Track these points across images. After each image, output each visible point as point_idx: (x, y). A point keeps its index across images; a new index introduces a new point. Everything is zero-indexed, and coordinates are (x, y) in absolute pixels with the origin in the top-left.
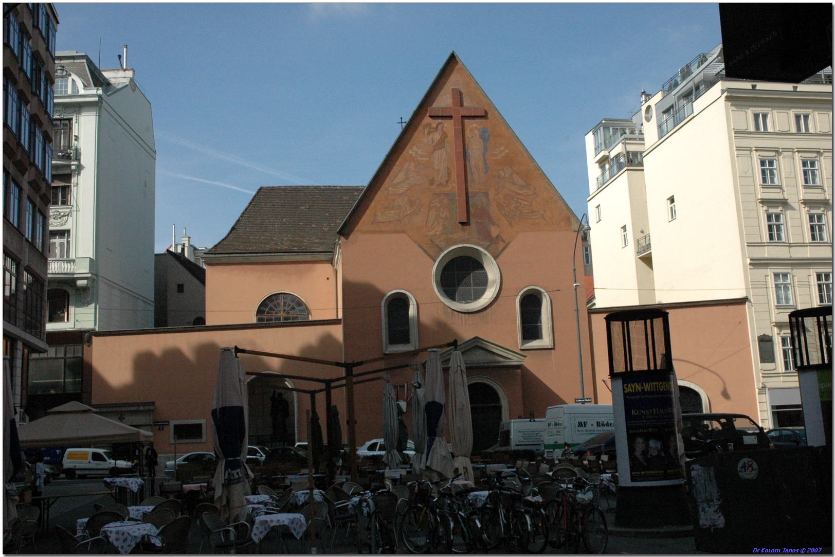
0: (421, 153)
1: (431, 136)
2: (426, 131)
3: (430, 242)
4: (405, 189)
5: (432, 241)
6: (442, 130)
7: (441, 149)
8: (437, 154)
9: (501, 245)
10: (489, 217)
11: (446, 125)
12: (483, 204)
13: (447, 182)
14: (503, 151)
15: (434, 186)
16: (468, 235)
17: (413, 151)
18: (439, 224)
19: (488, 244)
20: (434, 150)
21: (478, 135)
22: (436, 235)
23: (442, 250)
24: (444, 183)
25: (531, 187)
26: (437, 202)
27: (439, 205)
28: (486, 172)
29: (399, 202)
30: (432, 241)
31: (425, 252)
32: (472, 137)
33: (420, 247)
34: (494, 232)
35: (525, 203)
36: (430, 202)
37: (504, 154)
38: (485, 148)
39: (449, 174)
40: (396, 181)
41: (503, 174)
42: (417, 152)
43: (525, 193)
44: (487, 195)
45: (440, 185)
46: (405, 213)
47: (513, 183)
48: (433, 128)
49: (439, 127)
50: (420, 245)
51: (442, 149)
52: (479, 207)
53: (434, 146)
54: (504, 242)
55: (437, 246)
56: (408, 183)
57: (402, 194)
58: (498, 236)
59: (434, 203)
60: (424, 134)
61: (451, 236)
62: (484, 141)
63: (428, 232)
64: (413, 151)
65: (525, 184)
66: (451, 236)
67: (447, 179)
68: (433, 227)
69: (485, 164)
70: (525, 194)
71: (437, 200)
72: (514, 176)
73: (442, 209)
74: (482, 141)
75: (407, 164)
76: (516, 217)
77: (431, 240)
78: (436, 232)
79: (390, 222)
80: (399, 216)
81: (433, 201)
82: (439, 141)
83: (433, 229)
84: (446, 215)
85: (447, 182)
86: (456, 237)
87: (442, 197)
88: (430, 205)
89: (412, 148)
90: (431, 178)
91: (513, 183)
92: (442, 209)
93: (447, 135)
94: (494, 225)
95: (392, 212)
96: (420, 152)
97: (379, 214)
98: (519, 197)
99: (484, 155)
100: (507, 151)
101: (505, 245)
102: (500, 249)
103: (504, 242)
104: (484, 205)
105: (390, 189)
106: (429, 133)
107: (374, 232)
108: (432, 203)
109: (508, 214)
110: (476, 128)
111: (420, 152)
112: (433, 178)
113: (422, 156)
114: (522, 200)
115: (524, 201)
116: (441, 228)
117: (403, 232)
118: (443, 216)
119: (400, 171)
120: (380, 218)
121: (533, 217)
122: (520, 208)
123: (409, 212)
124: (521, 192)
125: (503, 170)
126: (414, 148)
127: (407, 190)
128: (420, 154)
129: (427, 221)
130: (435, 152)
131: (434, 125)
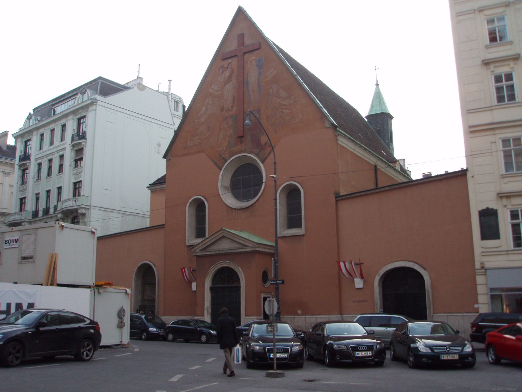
2: (221, 71)
5: (220, 155)
15: (224, 112)
19: (258, 151)
20: (225, 84)
21: (255, 65)
27: (226, 126)
28: (259, 93)
30: (220, 155)
32: (251, 67)
33: (213, 161)
34: (264, 139)
35: (288, 111)
39: (234, 101)
45: (228, 110)
49: (229, 67)
58: (265, 144)
61: (233, 149)
66: (233, 149)
67: (232, 105)
70: (287, 104)
85: (232, 107)
100: (275, 72)
105: (196, 120)
115: (287, 109)
124: (284, 103)
126: (213, 87)
131: (226, 66)
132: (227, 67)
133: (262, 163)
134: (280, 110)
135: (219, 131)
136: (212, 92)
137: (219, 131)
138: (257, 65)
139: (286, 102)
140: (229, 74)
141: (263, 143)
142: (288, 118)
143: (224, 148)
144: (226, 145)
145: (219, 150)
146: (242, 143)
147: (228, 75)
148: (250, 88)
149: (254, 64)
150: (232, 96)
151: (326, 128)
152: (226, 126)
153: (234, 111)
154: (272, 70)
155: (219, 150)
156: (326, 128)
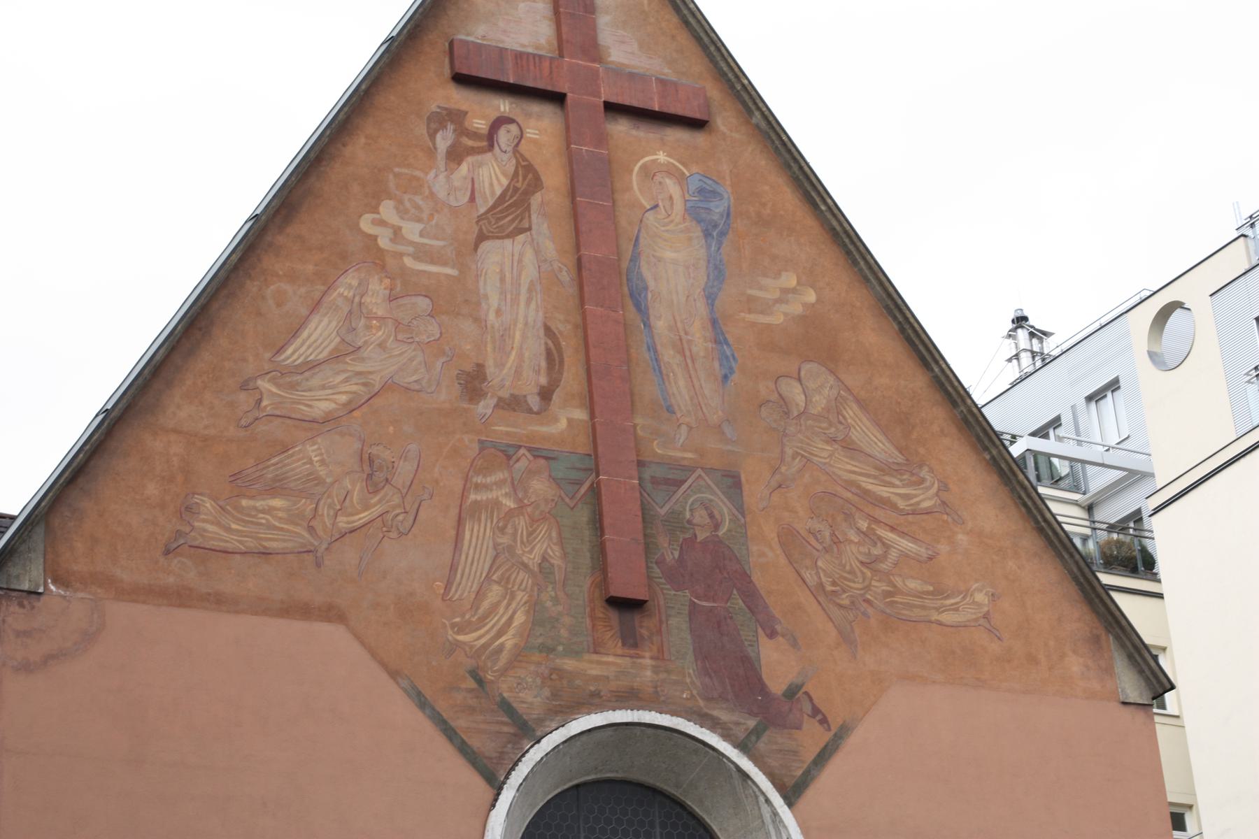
0: (417, 239)
1: (464, 168)
2: (444, 141)
3: (471, 684)
4: (343, 398)
5: (480, 682)
6: (516, 150)
7: (512, 235)
8: (495, 255)
9: (811, 738)
10: (751, 596)
11: (531, 133)
12: (717, 526)
13: (546, 394)
14: (794, 291)
15: (485, 407)
16: (656, 670)
17: (382, 223)
18: (513, 597)
19: (752, 723)
20: (481, 238)
21: (679, 206)
22: (501, 648)
23: (527, 732)
24: (534, 402)
25: (924, 473)
26: (500, 484)
27: (510, 503)
28: (725, 377)
29: (311, 462)
30: (480, 682)
31: (450, 733)
32: (656, 206)
33: (422, 703)
35: (906, 544)
36: (467, 479)
37: (796, 309)
38: (717, 272)
39: (553, 360)
40: (294, 354)
41: (800, 399)
42: (397, 231)
43: (906, 497)
44: (733, 483)
45: (513, 404)
46: (343, 522)
47: (850, 448)
48: (475, 135)
49: (505, 137)
50: (419, 694)
51: (521, 238)
52: (701, 536)
53: (480, 218)
54: (824, 721)
55: (506, 707)
56: (359, 374)
57: (328, 420)
58: (792, 692)
59: (486, 487)
60: (431, 152)
61: (569, 664)
62: (707, 234)
63: (461, 629)
64: (382, 223)
65: (900, 459)
66: (569, 664)
67: (543, 380)
68: (486, 605)
69: (719, 339)
70: (901, 504)
71: (499, 476)
72: (852, 412)
73: (522, 523)
74: (697, 232)
75: (351, 279)
76: (870, 611)
77: (475, 675)
78: (500, 634)
79: (266, 554)
80: (311, 529)
81: (479, 479)
82: (502, 198)
83: (483, 620)
84: (544, 559)
85: (546, 394)
86: (595, 671)
87: (522, 465)
88: (463, 496)
89: (375, 210)
90: (469, 367)
91: (850, 448)
92: (522, 523)
93: (537, 178)
94: (772, 634)
95: (277, 503)
96: (412, 230)
97: (209, 504)
98: (879, 513)
99: (710, 298)
100: (811, 297)
101: (828, 736)
102: (810, 754)
103: (824, 721)
104: (720, 533)
105: (264, 384)
106: (456, 155)
107: (181, 597)
108: (478, 487)
109: (829, 588)
110: (670, 171)
111: (412, 230)
112: (480, 367)
113: (423, 254)
114: (893, 529)
115: (903, 534)
116: (520, 618)
117: (332, 614)
118: (533, 558)
119: (315, 307)
120: (210, 527)
121: (947, 618)
122: (884, 566)
123: (364, 516)
124: (884, 492)
125: (799, 380)
126: (387, 210)
127: (351, 408)
128: (411, 243)
129: (453, 568)
130: (486, 245)
131: (480, 124)
132: (491, 138)
133: (790, 804)
134: (864, 525)
135: (460, 522)
136: (384, 243)
137: (460, 522)
138: (693, 213)
139: (892, 490)
140: (505, 182)
141: (777, 686)
142: (913, 584)
143: (509, 641)
144: (516, 623)
145: (461, 638)
146: (631, 641)
147: (498, 191)
148: (660, 325)
149: (671, 198)
150: (540, 324)
151: (1124, 703)
152: (510, 503)
153: (563, 424)
154: (790, 280)
155: (461, 638)
156: (1124, 703)
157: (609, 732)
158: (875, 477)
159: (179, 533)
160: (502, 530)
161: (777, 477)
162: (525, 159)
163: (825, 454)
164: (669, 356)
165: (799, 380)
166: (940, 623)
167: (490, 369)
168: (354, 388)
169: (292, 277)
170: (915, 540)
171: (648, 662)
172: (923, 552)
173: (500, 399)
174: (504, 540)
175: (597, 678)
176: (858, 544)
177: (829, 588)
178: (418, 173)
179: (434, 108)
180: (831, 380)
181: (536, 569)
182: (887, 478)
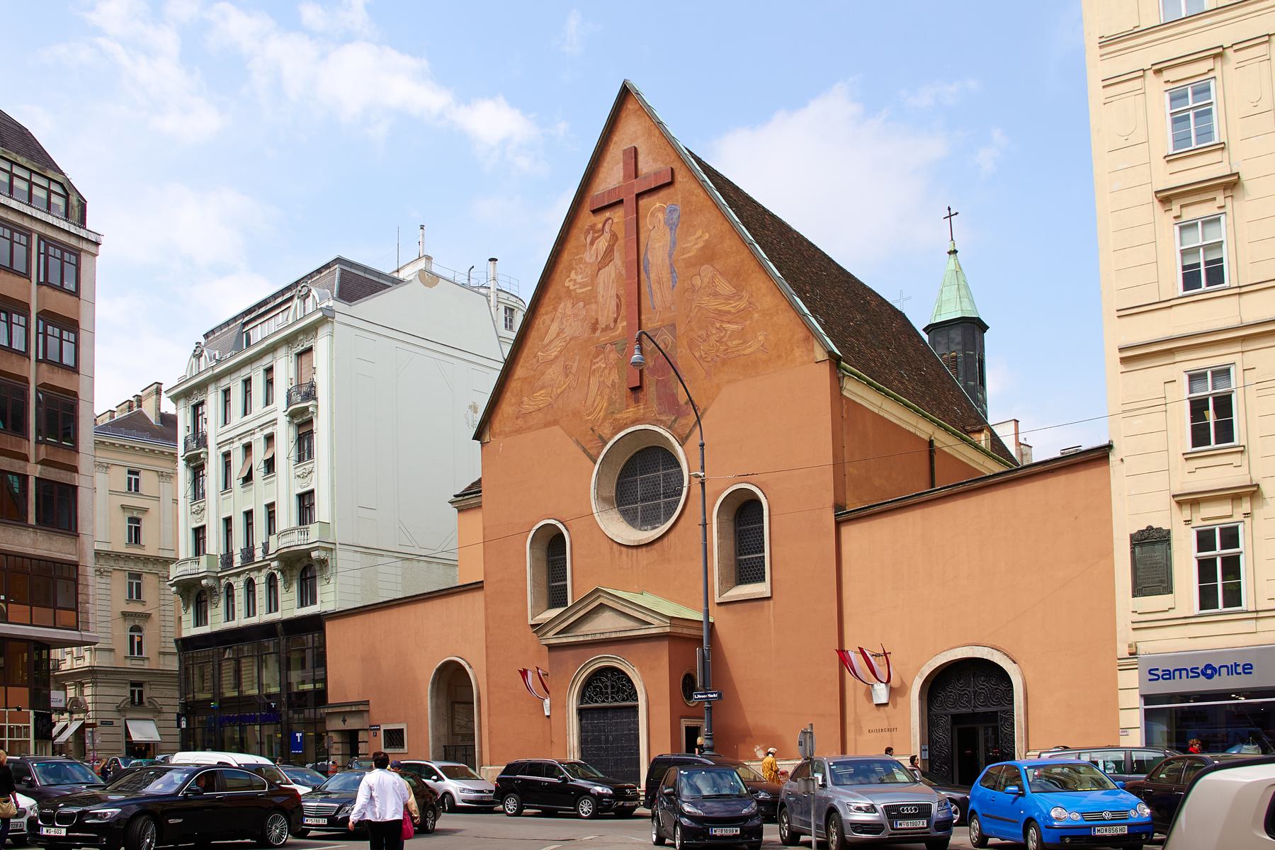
16: (644, 409)
19: (673, 418)
35: (734, 327)
37: (701, 244)
57: (556, 357)
59: (598, 362)
61: (618, 416)
63: (588, 415)
66: (618, 416)
70: (733, 310)
85: (615, 321)
93: (617, 237)
98: (724, 318)
100: (707, 236)
114: (729, 322)
118: (609, 383)
121: (746, 352)
124: (727, 308)
134: (718, 325)
140: (606, 244)
146: (637, 401)
148: (652, 276)
152: (604, 365)
157: (629, 436)
158: (724, 303)
159: (519, 411)
160: (601, 376)
161: (689, 319)
162: (613, 232)
163: (706, 302)
164: (655, 286)
165: (700, 275)
166: (744, 355)
167: (600, 319)
168: (563, 344)
169: (547, 313)
170: (737, 323)
171: (642, 407)
172: (740, 327)
173: (602, 329)
174: (601, 379)
175: (626, 418)
176: (716, 334)
177: (704, 356)
178: (581, 256)
179: (587, 227)
180: (711, 268)
181: (610, 386)
182: (729, 302)
